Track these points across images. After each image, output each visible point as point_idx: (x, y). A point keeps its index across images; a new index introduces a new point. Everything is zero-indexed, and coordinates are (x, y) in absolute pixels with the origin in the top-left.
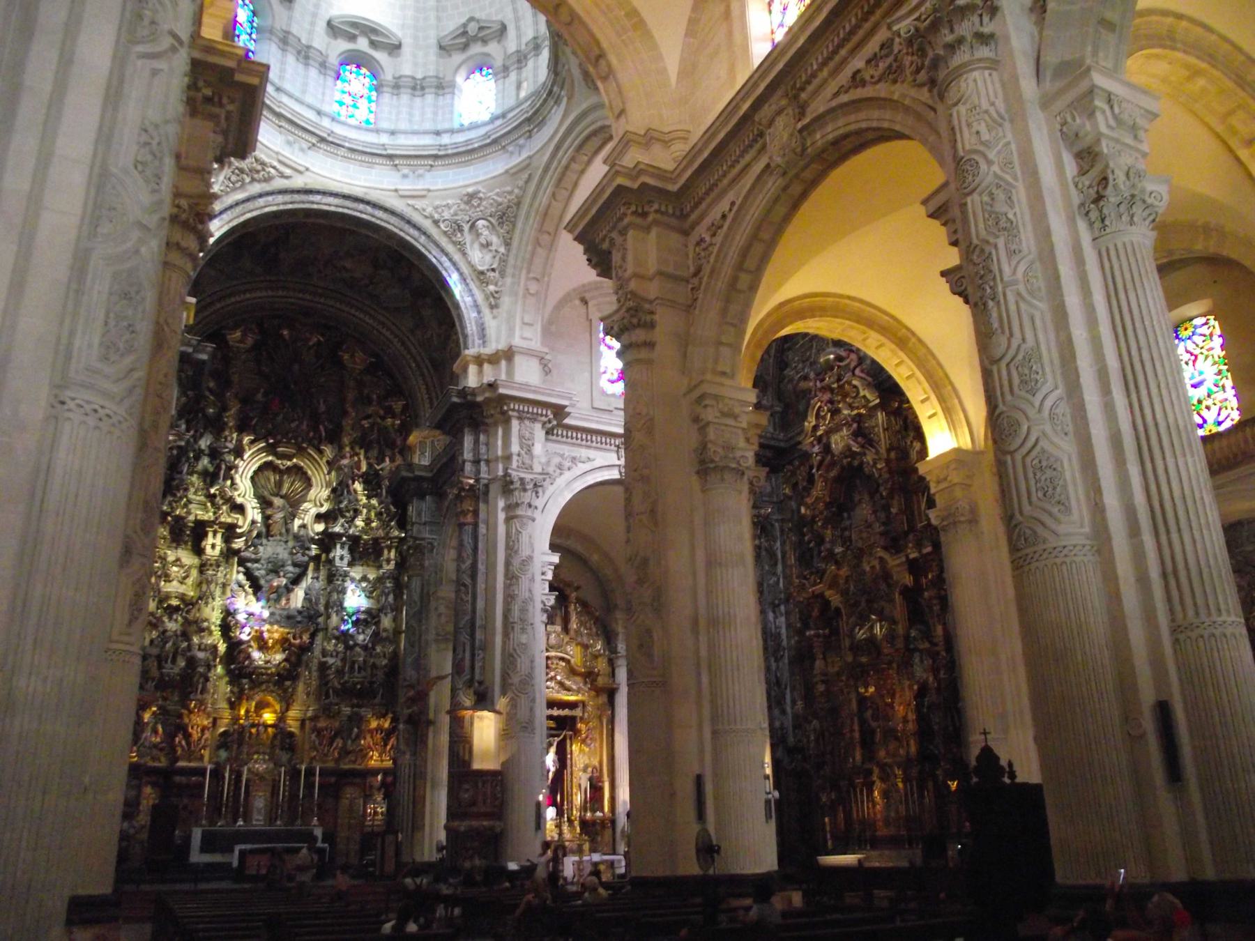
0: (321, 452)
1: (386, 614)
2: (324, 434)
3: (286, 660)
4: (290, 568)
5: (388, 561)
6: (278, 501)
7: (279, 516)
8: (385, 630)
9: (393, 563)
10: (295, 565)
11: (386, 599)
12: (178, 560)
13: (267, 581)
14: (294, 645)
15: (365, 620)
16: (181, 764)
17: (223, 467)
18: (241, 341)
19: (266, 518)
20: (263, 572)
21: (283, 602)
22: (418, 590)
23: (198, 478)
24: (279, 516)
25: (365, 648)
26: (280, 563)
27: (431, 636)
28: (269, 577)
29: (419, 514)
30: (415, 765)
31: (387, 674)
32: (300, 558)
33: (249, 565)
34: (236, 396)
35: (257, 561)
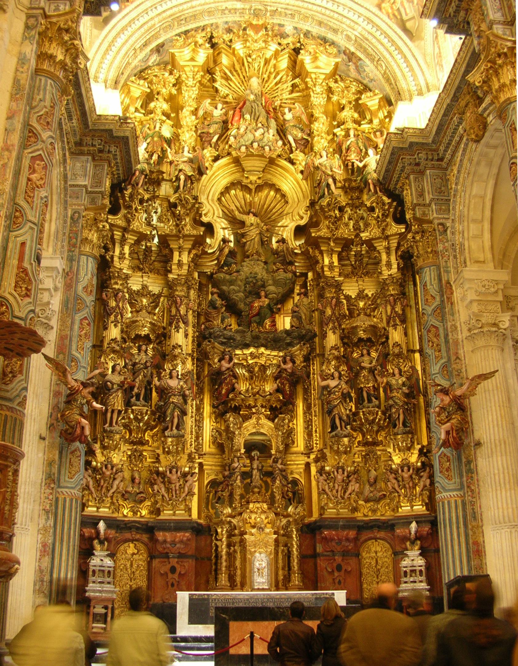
0: (292, 162)
1: (395, 326)
2: (293, 145)
3: (278, 390)
4: (272, 288)
5: (389, 265)
6: (251, 219)
7: (253, 233)
8: (396, 345)
9: (395, 266)
10: (276, 283)
11: (393, 309)
12: (144, 287)
13: (245, 304)
14: (285, 370)
15: (369, 340)
16: (167, 514)
17: (182, 177)
18: (192, 59)
19: (239, 237)
20: (241, 295)
21: (268, 322)
22: (435, 283)
23: (161, 205)
24: (253, 233)
25: (372, 371)
26: (260, 283)
27: (462, 334)
28: (249, 300)
29: (421, 194)
30: (464, 504)
31: (407, 395)
32: (281, 275)
33: (225, 288)
34: (195, 112)
35: (232, 283)
